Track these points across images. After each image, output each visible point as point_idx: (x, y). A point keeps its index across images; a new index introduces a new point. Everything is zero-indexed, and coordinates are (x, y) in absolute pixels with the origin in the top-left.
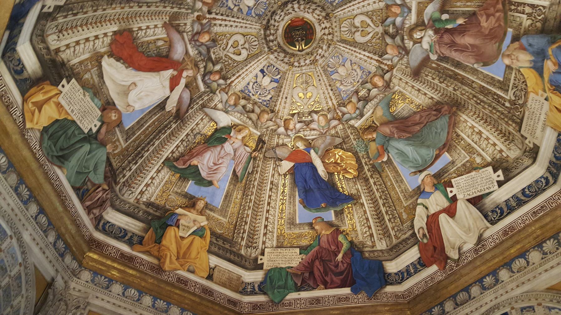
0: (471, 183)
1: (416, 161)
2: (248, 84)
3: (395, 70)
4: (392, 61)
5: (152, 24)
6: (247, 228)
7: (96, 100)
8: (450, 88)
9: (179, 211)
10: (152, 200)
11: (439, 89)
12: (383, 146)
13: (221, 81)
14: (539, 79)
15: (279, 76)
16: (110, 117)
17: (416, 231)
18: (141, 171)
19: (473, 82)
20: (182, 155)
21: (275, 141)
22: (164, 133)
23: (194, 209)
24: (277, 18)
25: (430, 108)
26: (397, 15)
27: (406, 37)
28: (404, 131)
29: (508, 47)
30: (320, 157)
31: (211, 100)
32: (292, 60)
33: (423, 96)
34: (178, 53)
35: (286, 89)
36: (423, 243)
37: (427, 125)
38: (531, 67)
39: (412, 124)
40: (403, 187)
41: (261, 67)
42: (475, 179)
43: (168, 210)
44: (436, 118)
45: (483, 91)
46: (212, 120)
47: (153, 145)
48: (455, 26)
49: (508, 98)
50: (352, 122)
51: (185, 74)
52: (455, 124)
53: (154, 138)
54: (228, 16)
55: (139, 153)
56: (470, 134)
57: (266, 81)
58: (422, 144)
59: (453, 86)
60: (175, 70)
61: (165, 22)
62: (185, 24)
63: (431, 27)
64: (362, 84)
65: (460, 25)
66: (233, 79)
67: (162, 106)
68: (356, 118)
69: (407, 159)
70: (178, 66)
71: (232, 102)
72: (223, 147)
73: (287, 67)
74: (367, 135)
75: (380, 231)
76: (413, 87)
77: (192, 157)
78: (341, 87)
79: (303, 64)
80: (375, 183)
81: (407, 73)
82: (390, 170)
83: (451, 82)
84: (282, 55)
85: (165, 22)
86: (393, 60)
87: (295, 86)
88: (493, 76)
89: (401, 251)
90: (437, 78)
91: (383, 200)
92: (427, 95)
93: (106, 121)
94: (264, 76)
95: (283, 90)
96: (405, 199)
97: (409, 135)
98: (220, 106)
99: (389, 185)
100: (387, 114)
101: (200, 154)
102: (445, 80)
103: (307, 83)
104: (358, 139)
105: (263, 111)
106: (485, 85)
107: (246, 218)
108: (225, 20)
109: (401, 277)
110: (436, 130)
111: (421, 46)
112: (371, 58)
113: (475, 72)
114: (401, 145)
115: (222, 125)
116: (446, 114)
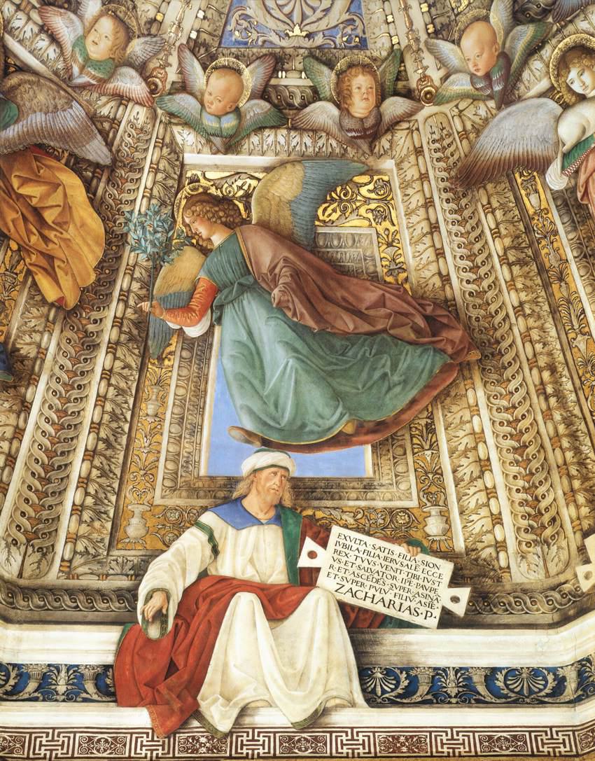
0: (378, 568)
1: (276, 406)
4: (445, 78)
8: (513, 293)
11: (482, 271)
17: (142, 592)
28: (309, 302)
33: (430, 254)
36: (143, 633)
37: (379, 337)
39: (344, 299)
40: (187, 447)
42: (394, 566)
44: (413, 336)
52: (446, 393)
56: (461, 448)
58: (326, 377)
59: (523, 296)
69: (256, 383)
75: (24, 520)
76: (429, 203)
81: (448, 152)
82: (184, 372)
83: (529, 283)
86: (453, 77)
89: (58, 615)
90: (507, 241)
91: (99, 439)
92: (441, 260)
96: (168, 483)
99: (150, 412)
109: (12, 682)
110: (388, 370)
116: (443, 351)
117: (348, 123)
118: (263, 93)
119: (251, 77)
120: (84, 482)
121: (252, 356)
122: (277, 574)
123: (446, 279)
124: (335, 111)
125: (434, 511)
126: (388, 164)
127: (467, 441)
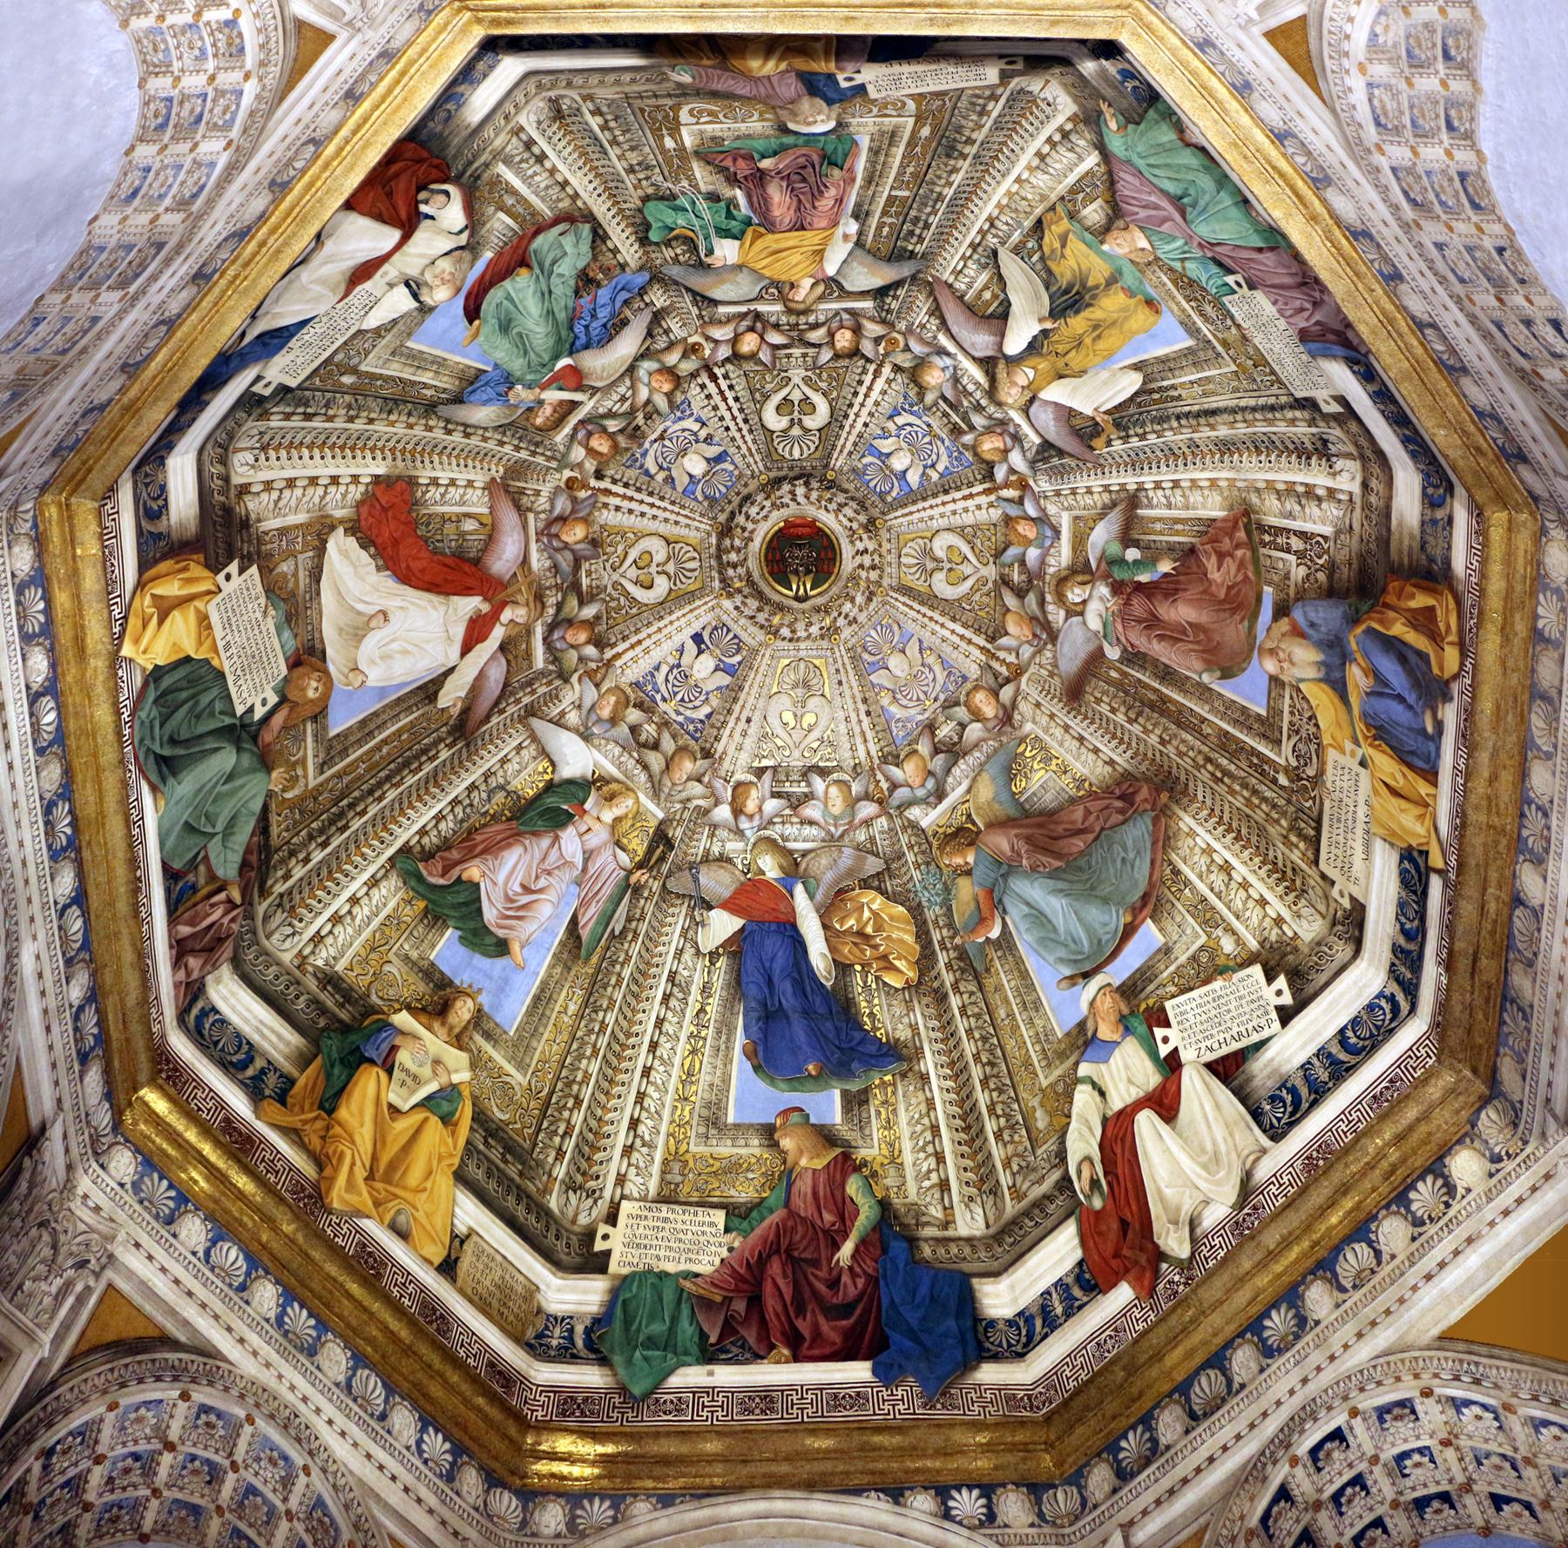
7: (287, 634)
12: (991, 892)
16: (304, 690)
20: (446, 845)
22: (415, 772)
47: (380, 799)
53: (388, 778)
72: (557, 838)
74: (950, 854)
76: (1067, 728)
77: (470, 855)
93: (291, 696)
100: (1005, 797)
101: (493, 849)
104: (928, 864)
117: (990, 725)
118: (936, 751)
119: (924, 748)
124: (978, 725)
126: (1028, 727)
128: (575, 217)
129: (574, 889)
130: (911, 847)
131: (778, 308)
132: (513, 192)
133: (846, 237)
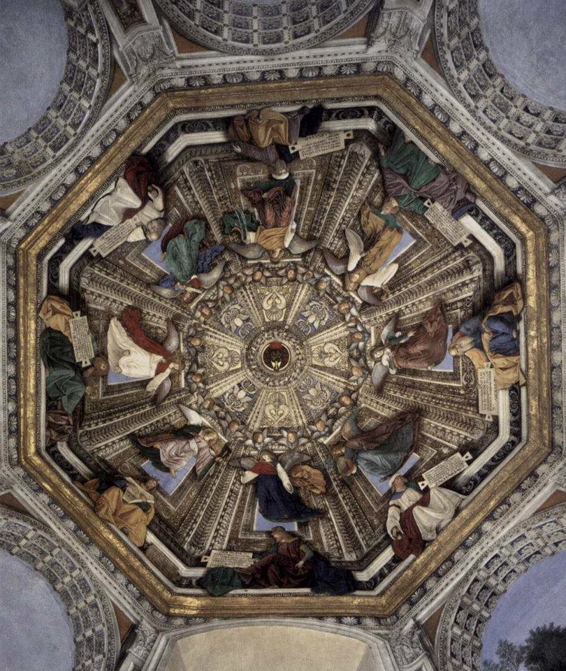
2: (225, 393)
3: (360, 390)
5: (158, 315)
6: (196, 527)
9: (129, 479)
10: (107, 458)
13: (201, 385)
14: (481, 353)
15: (254, 392)
18: (106, 432)
19: (430, 384)
20: (148, 435)
21: (242, 451)
23: (145, 485)
24: (259, 340)
25: (393, 419)
26: (360, 340)
27: (368, 358)
29: (452, 340)
30: (286, 471)
31: (187, 399)
32: (267, 380)
33: (388, 410)
34: (173, 344)
35: (258, 404)
38: (472, 348)
41: (239, 381)
43: (118, 473)
45: (440, 389)
46: (184, 415)
47: (125, 415)
48: (407, 339)
49: (461, 385)
50: (322, 440)
51: (172, 365)
54: (219, 330)
55: (110, 414)
57: (242, 394)
60: (164, 358)
61: (168, 318)
62: (184, 326)
63: (388, 346)
64: (331, 404)
65: (411, 337)
66: (211, 386)
67: (144, 383)
68: (324, 436)
70: (169, 357)
71: (206, 406)
72: (188, 443)
73: (262, 385)
74: (335, 451)
76: (378, 403)
77: (156, 440)
78: (312, 407)
79: (277, 384)
80: (344, 498)
84: (259, 374)
85: (168, 318)
87: (268, 402)
88: (445, 371)
94: (240, 389)
95: (256, 405)
97: (376, 445)
98: (194, 406)
102: (405, 391)
103: (279, 401)
105: (234, 421)
106: (440, 383)
107: (197, 517)
108: (216, 333)
111: (382, 364)
112: (339, 381)
113: (430, 374)
114: (369, 456)
115: (192, 422)
120: (357, 525)
121: (371, 464)
122: (417, 496)
123: (396, 410)
125: (442, 448)
127: (434, 430)
128: (200, 218)
129: (195, 460)
130: (320, 451)
131: (268, 261)
132: (180, 201)
133: (292, 230)
